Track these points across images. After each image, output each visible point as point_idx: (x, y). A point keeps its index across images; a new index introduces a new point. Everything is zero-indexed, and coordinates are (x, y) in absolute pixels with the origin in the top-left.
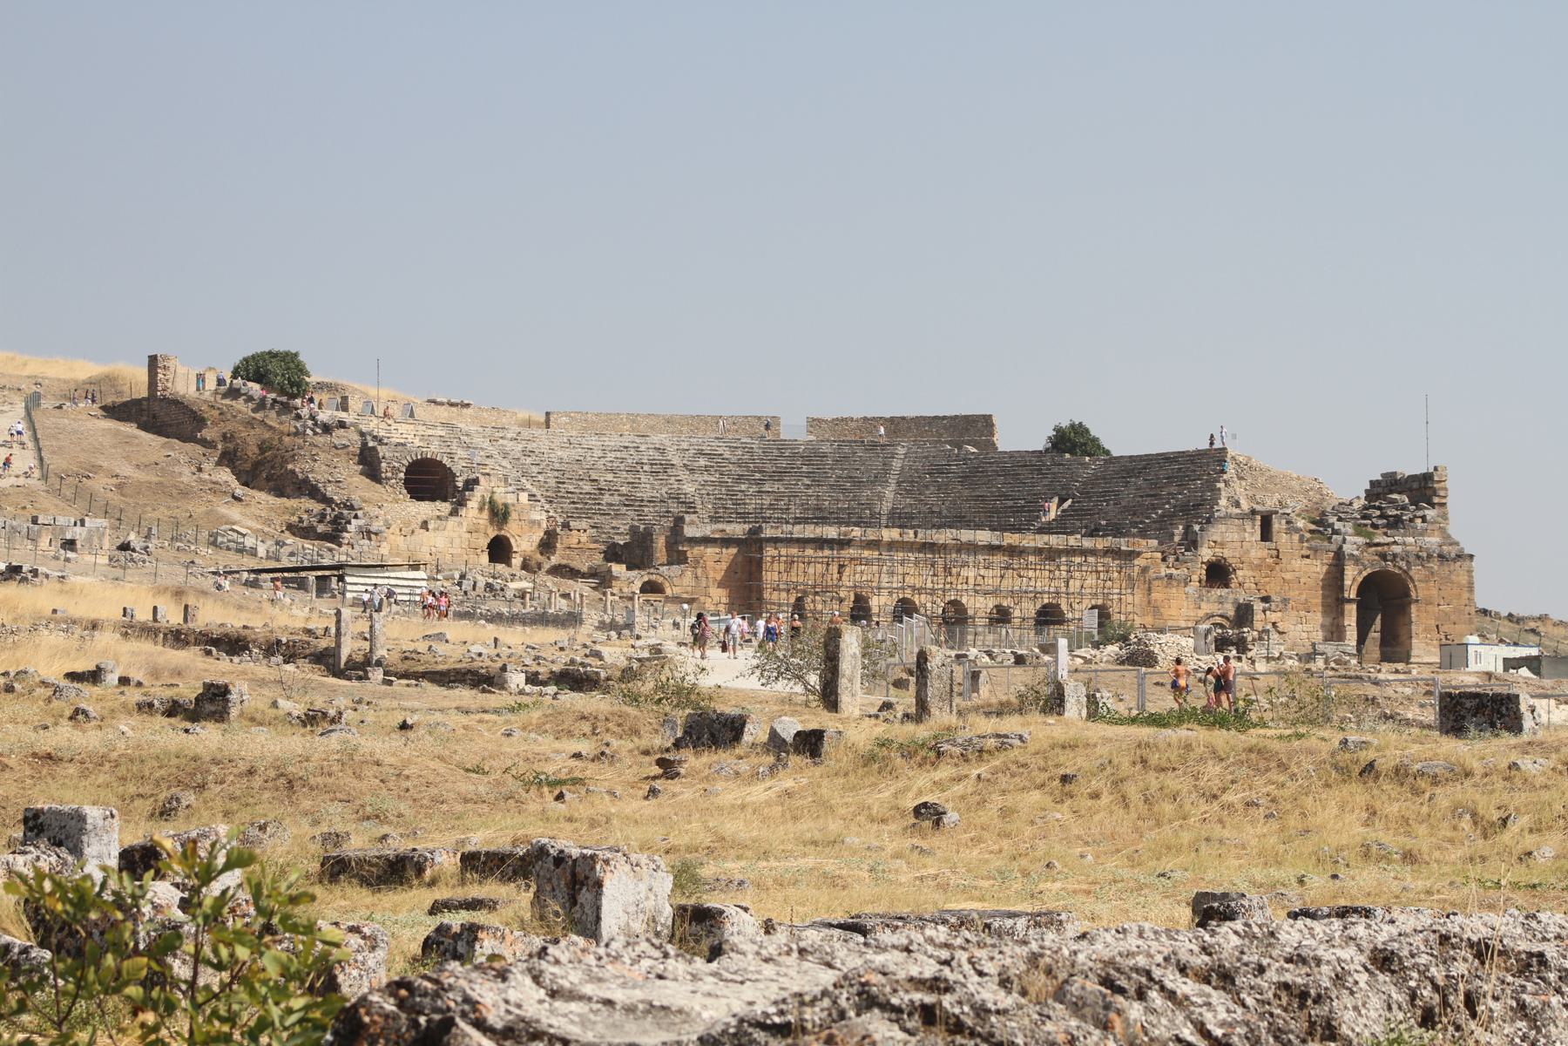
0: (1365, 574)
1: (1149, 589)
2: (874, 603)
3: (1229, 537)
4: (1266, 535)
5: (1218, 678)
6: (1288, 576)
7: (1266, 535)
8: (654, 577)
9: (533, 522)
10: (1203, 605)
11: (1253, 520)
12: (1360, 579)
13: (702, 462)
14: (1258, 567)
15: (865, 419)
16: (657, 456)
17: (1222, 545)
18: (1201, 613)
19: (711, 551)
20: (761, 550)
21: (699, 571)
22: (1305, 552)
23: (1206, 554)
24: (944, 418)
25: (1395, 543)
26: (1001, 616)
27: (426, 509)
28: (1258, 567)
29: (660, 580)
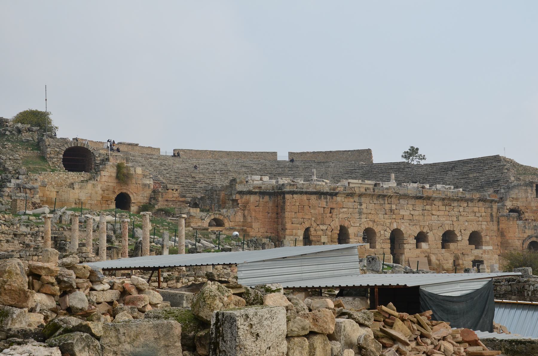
2: (351, 231)
8: (217, 216)
9: (145, 185)
10: (527, 231)
11: (532, 187)
13: (244, 169)
15: (314, 153)
16: (223, 167)
17: (517, 199)
18: (526, 236)
19: (253, 198)
20: (284, 198)
21: (246, 212)
23: (509, 204)
24: (349, 151)
26: (421, 238)
27: (73, 176)
29: (221, 218)
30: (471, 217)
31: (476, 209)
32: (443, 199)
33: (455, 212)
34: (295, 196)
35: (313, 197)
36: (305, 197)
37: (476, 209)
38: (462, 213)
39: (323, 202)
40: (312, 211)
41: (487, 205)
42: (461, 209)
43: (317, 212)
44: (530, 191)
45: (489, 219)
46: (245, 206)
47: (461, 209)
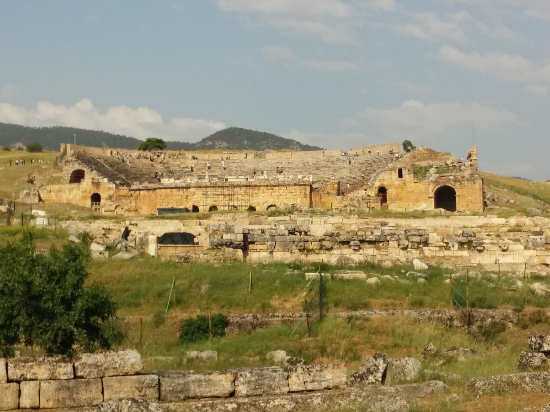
0: (437, 187)
1: (321, 197)
3: (385, 177)
4: (400, 176)
5: (341, 227)
6: (409, 190)
7: (400, 176)
11: (395, 171)
12: (435, 189)
14: (397, 188)
17: (384, 180)
21: (138, 201)
22: (415, 181)
25: (451, 175)
28: (397, 188)
30: (289, 195)
31: (293, 191)
32: (267, 186)
33: (277, 193)
34: (162, 190)
35: (174, 190)
36: (169, 190)
37: (293, 191)
38: (282, 194)
39: (181, 192)
40: (174, 198)
41: (303, 187)
42: (281, 191)
43: (177, 198)
44: (393, 174)
45: (303, 196)
46: (137, 197)
47: (281, 191)
